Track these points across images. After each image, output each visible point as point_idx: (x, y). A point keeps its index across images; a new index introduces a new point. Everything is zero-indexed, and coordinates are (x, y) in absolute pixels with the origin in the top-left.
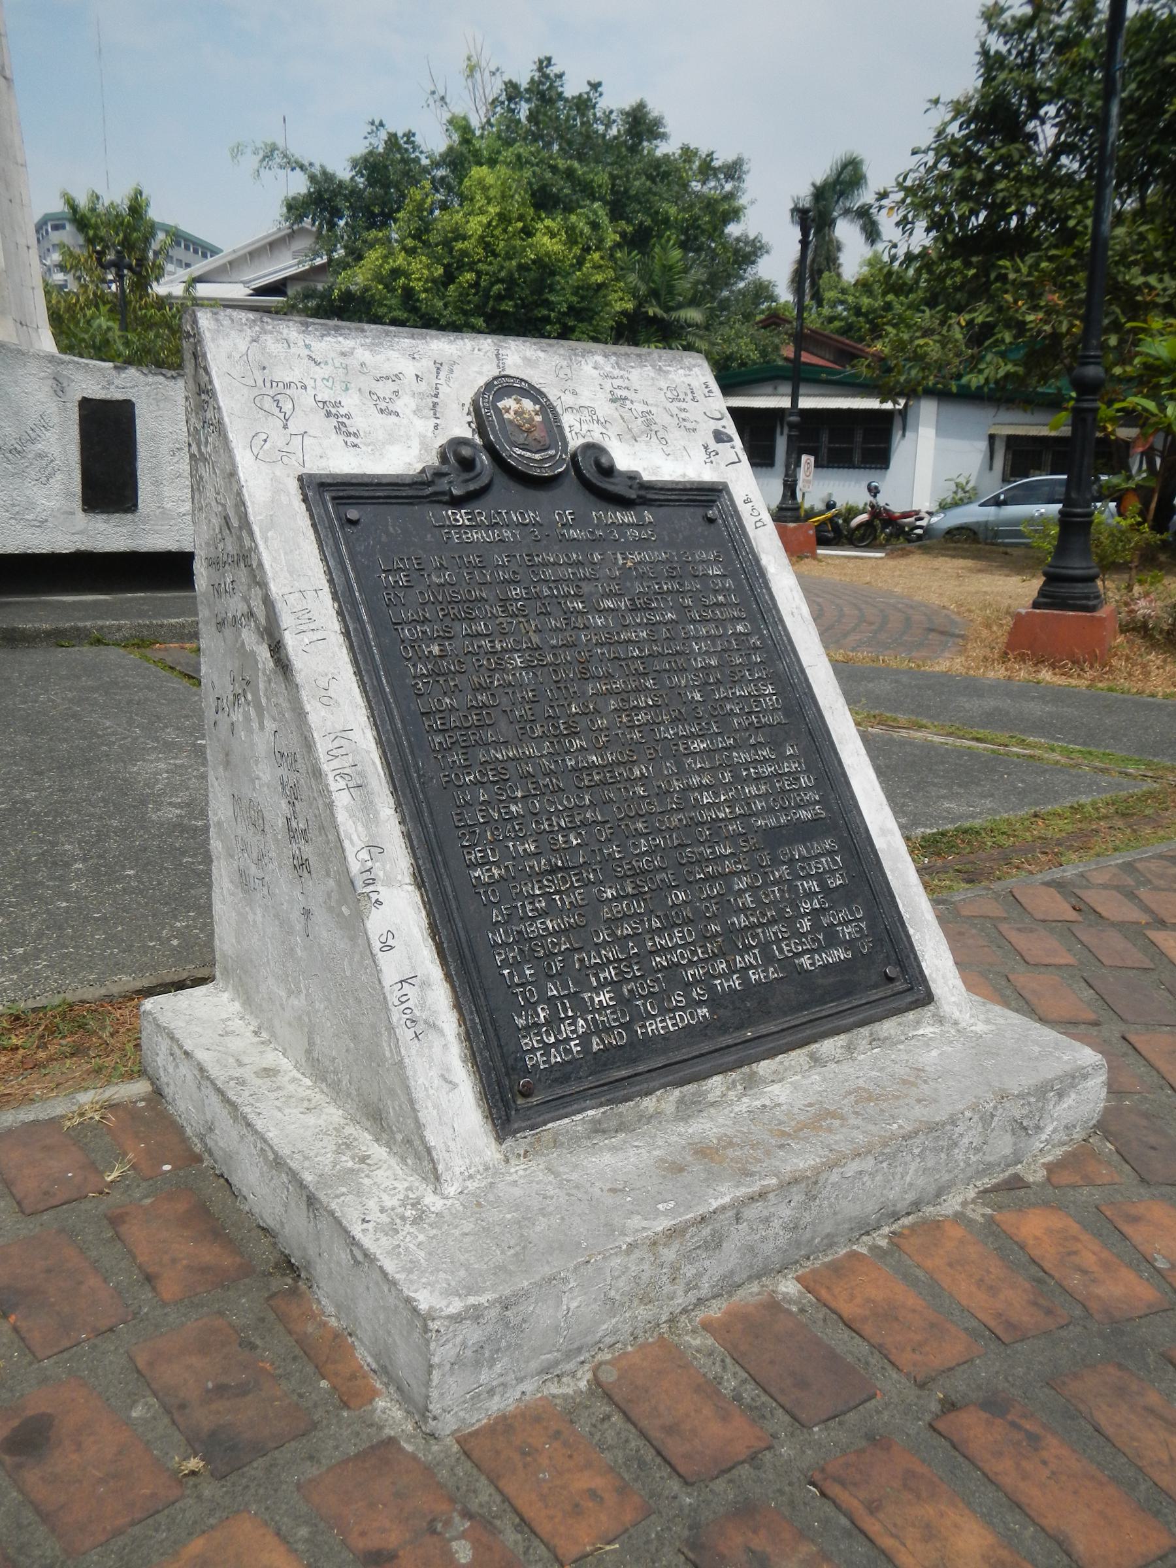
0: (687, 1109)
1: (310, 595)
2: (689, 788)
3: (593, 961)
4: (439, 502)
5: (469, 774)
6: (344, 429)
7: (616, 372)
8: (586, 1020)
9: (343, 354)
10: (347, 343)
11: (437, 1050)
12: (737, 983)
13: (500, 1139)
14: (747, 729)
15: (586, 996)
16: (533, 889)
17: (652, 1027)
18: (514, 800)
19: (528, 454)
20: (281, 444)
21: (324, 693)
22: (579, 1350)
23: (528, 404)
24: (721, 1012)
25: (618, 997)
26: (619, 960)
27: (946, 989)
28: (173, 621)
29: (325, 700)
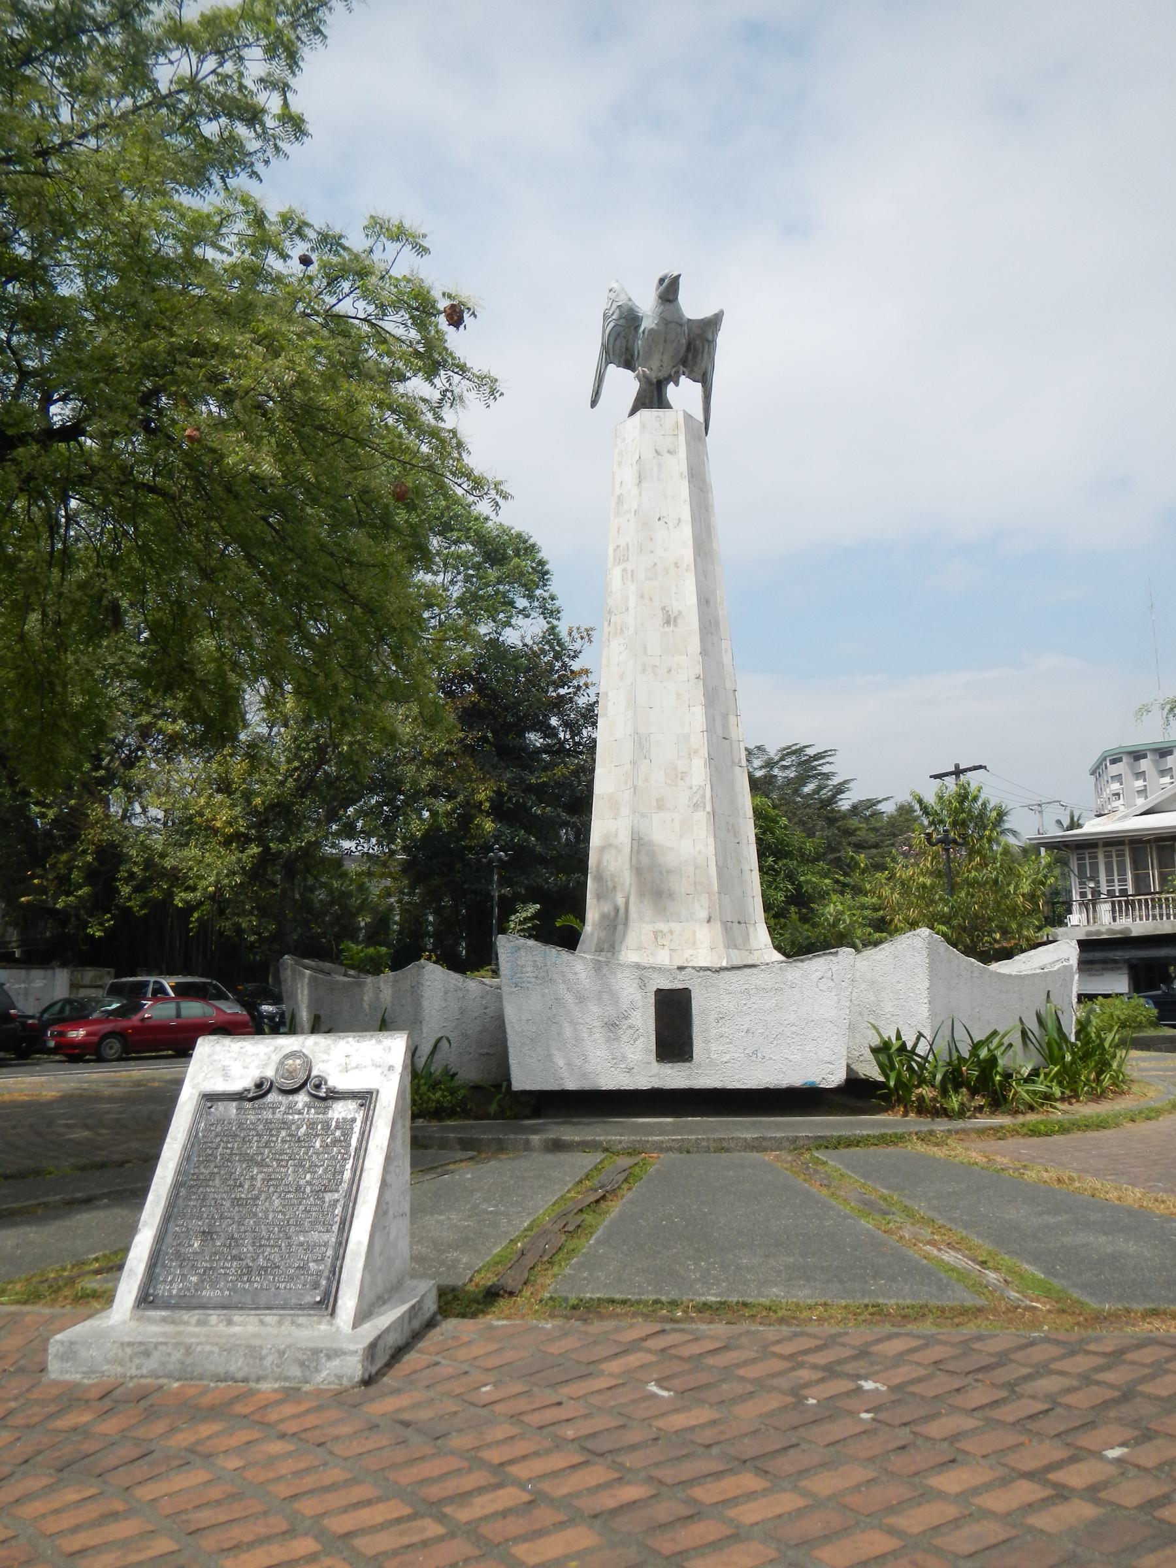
0: (201, 1323)
10: (240, 1044)
22: (96, 1372)
23: (298, 1062)
28: (656, 1138)
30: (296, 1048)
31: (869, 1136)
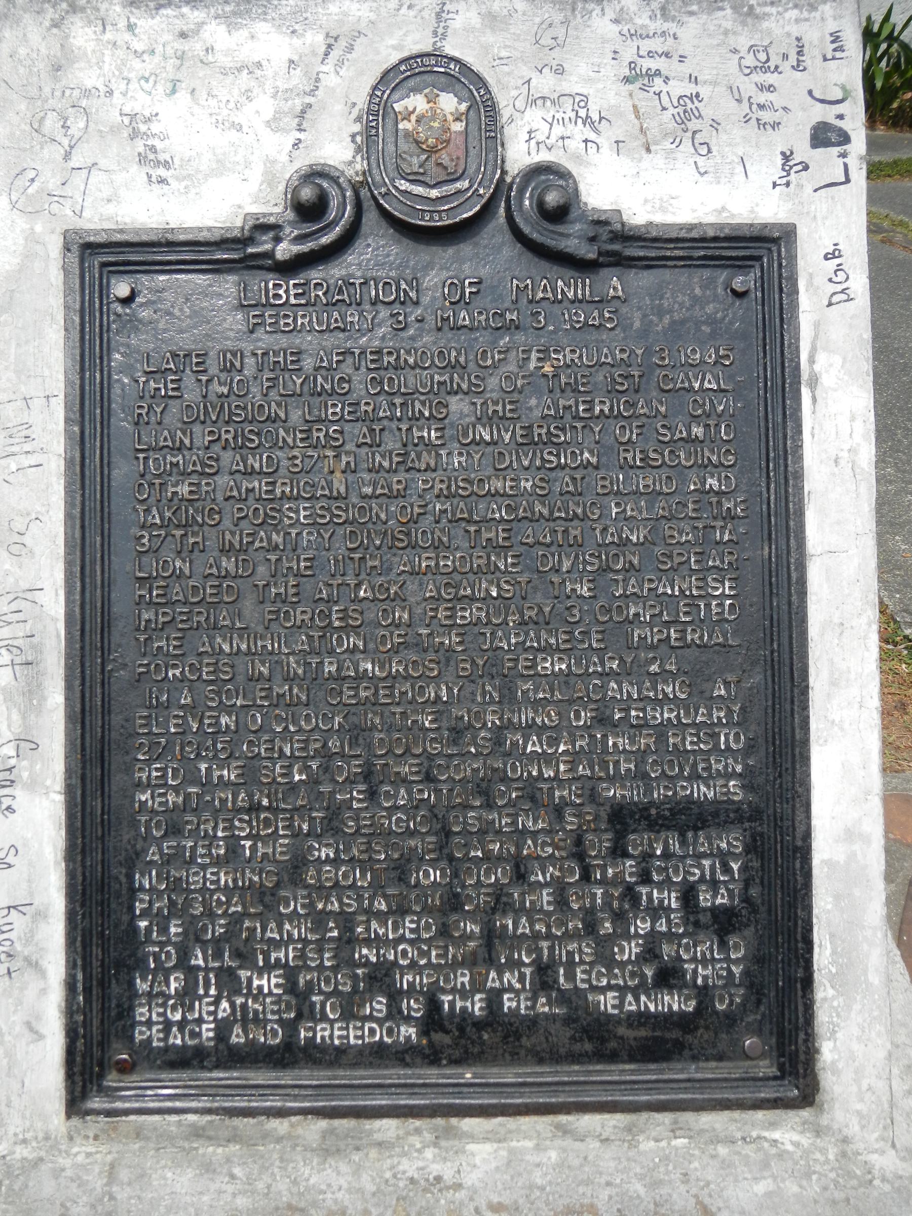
1: (37, 404)
2: (509, 726)
3: (269, 934)
4: (260, 268)
5: (175, 666)
6: (151, 156)
7: (658, 25)
8: (233, 1005)
9: (183, 35)
11: (31, 993)
12: (477, 1006)
13: (69, 1116)
14: (653, 647)
15: (244, 974)
16: (215, 828)
17: (322, 1032)
18: (229, 710)
19: (419, 190)
20: (53, 184)
21: (17, 538)
23: (448, 103)
24: (437, 1037)
25: (291, 986)
26: (305, 941)
27: (854, 1089)
29: (15, 549)
30: (418, 41)
31: (880, 163)
